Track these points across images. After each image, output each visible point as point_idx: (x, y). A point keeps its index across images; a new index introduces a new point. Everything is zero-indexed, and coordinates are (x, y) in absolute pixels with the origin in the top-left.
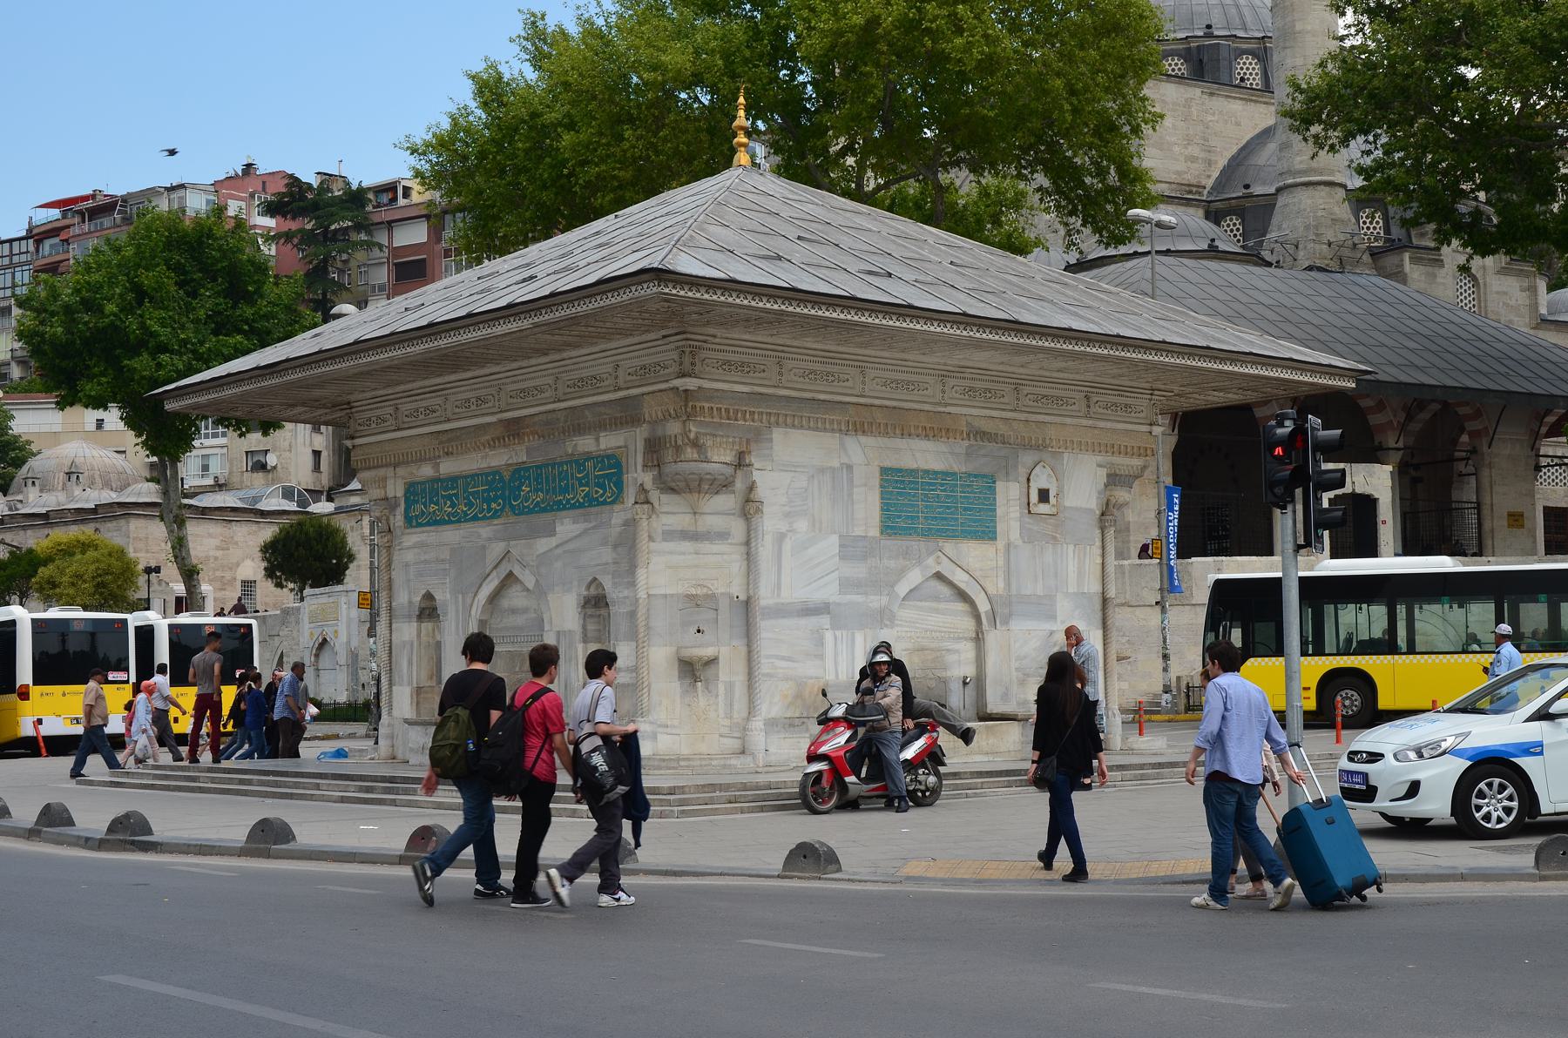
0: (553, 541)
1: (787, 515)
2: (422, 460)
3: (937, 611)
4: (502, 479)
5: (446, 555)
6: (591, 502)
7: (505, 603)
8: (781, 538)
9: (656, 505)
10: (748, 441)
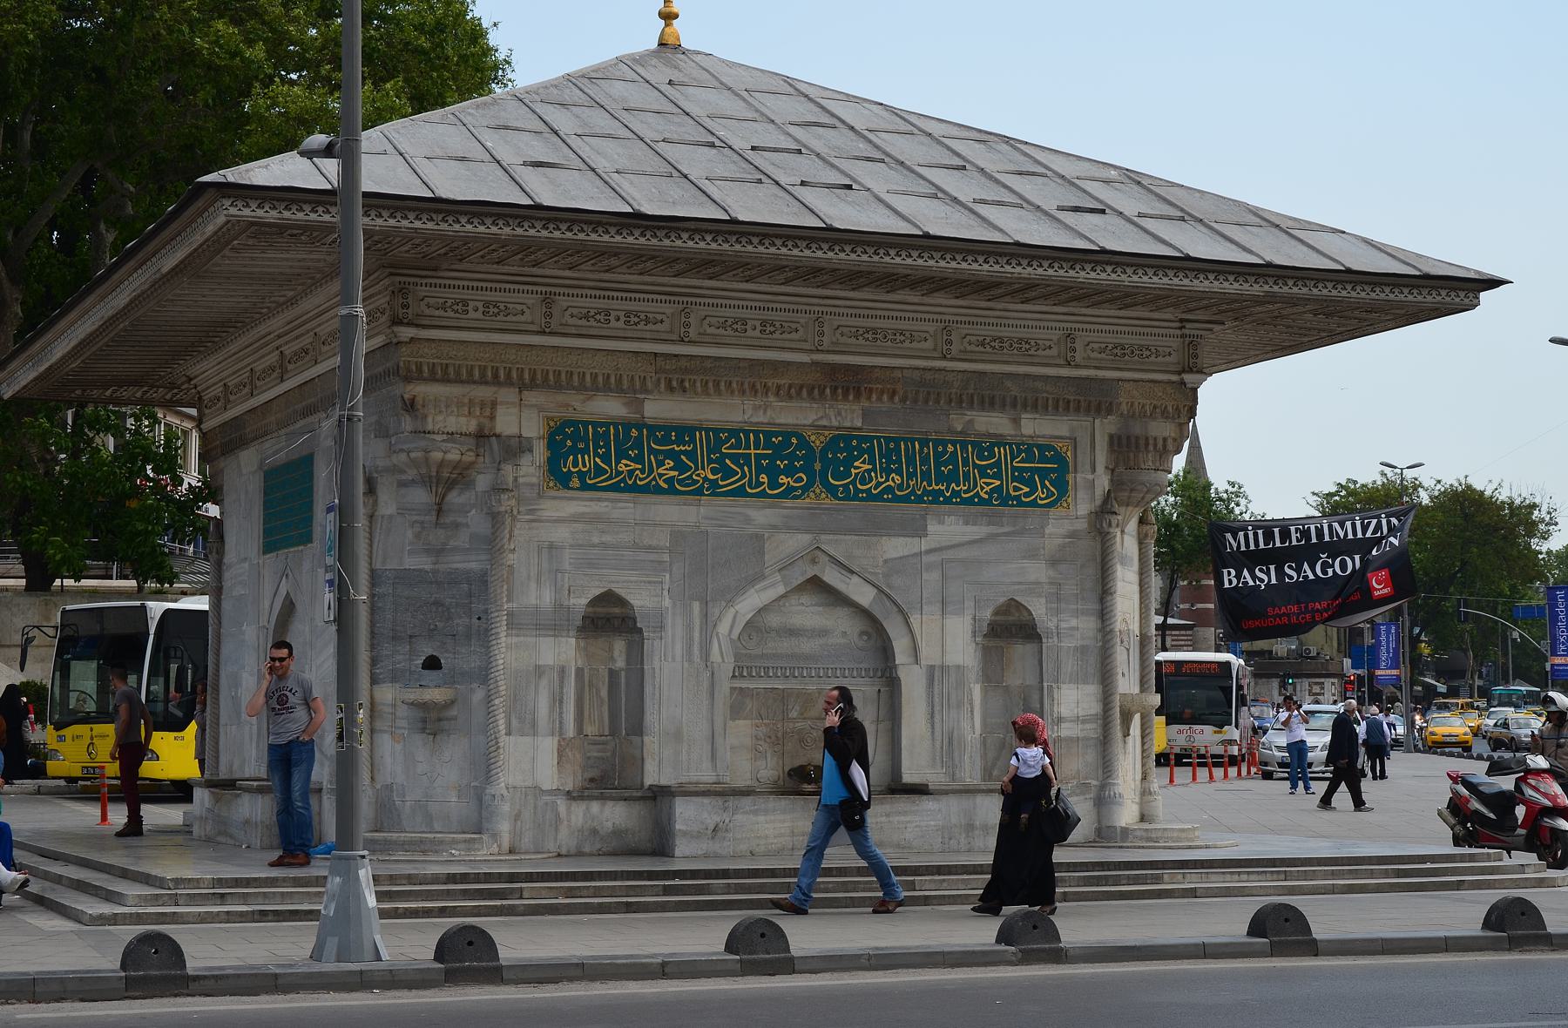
0: (925, 544)
2: (605, 387)
4: (804, 443)
5: (664, 540)
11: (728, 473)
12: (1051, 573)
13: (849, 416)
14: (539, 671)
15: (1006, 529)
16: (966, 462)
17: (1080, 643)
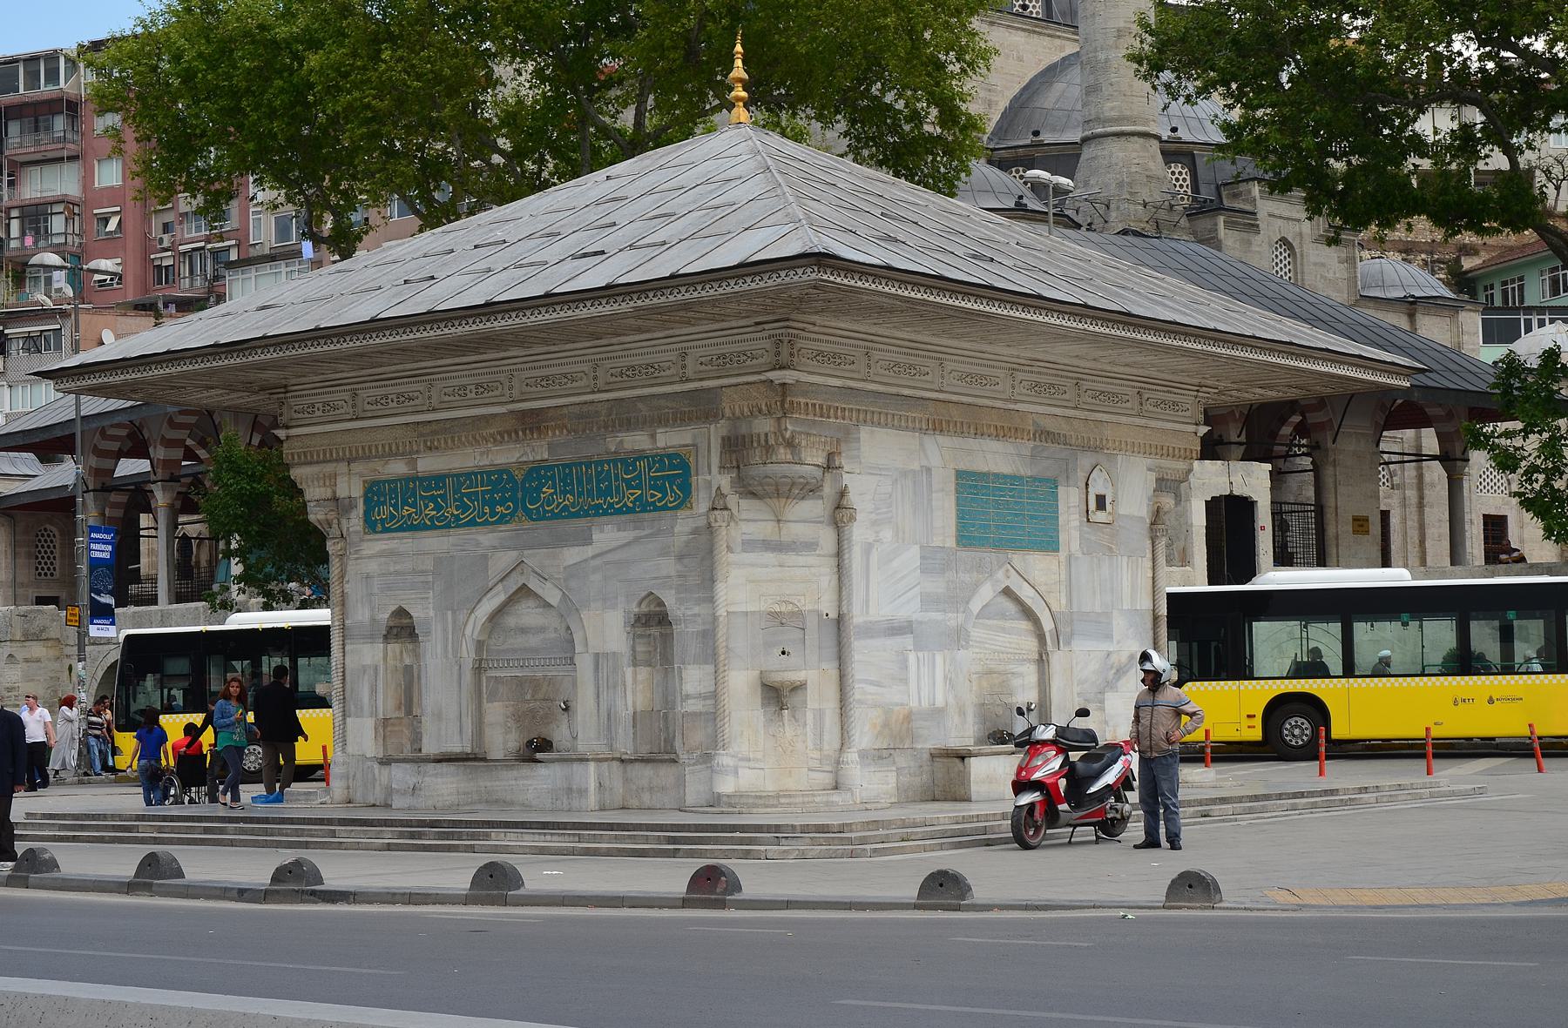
0: (589, 551)
1: (874, 523)
2: (390, 454)
3: (1003, 630)
4: (511, 478)
5: (429, 564)
6: (644, 506)
7: (510, 621)
9: (735, 511)
10: (838, 441)
11: (465, 508)
12: (679, 567)
13: (537, 451)
14: (364, 669)
15: (647, 532)
16: (616, 475)
17: (701, 628)
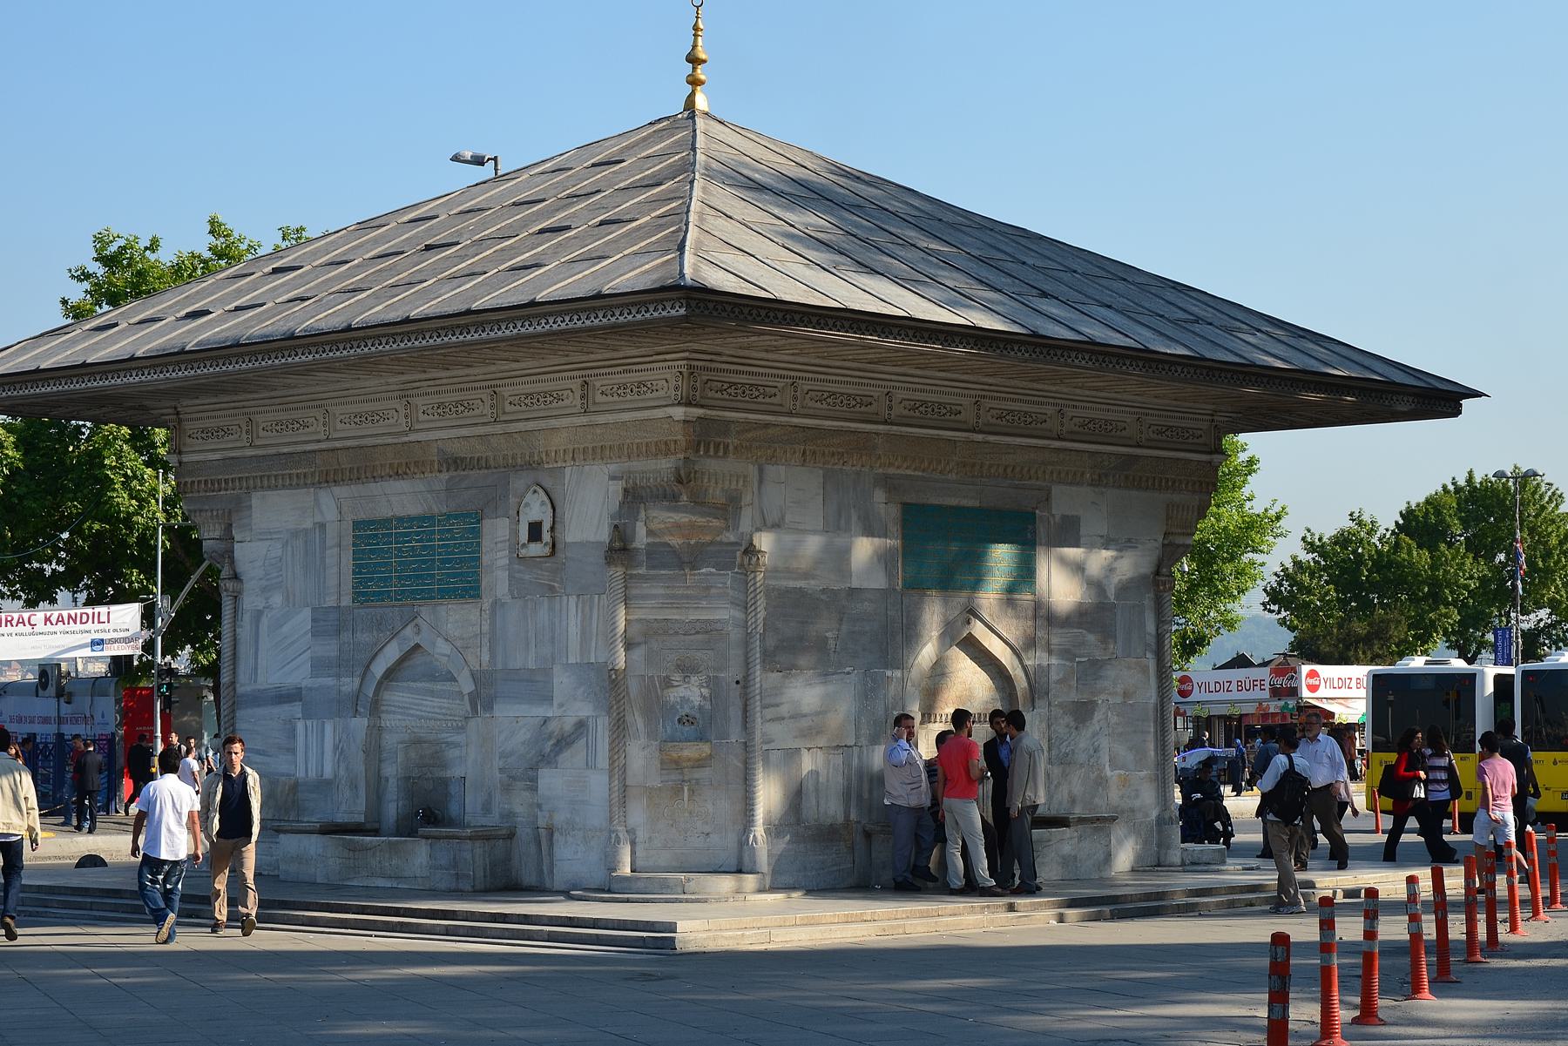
3: (432, 693)
8: (258, 615)
